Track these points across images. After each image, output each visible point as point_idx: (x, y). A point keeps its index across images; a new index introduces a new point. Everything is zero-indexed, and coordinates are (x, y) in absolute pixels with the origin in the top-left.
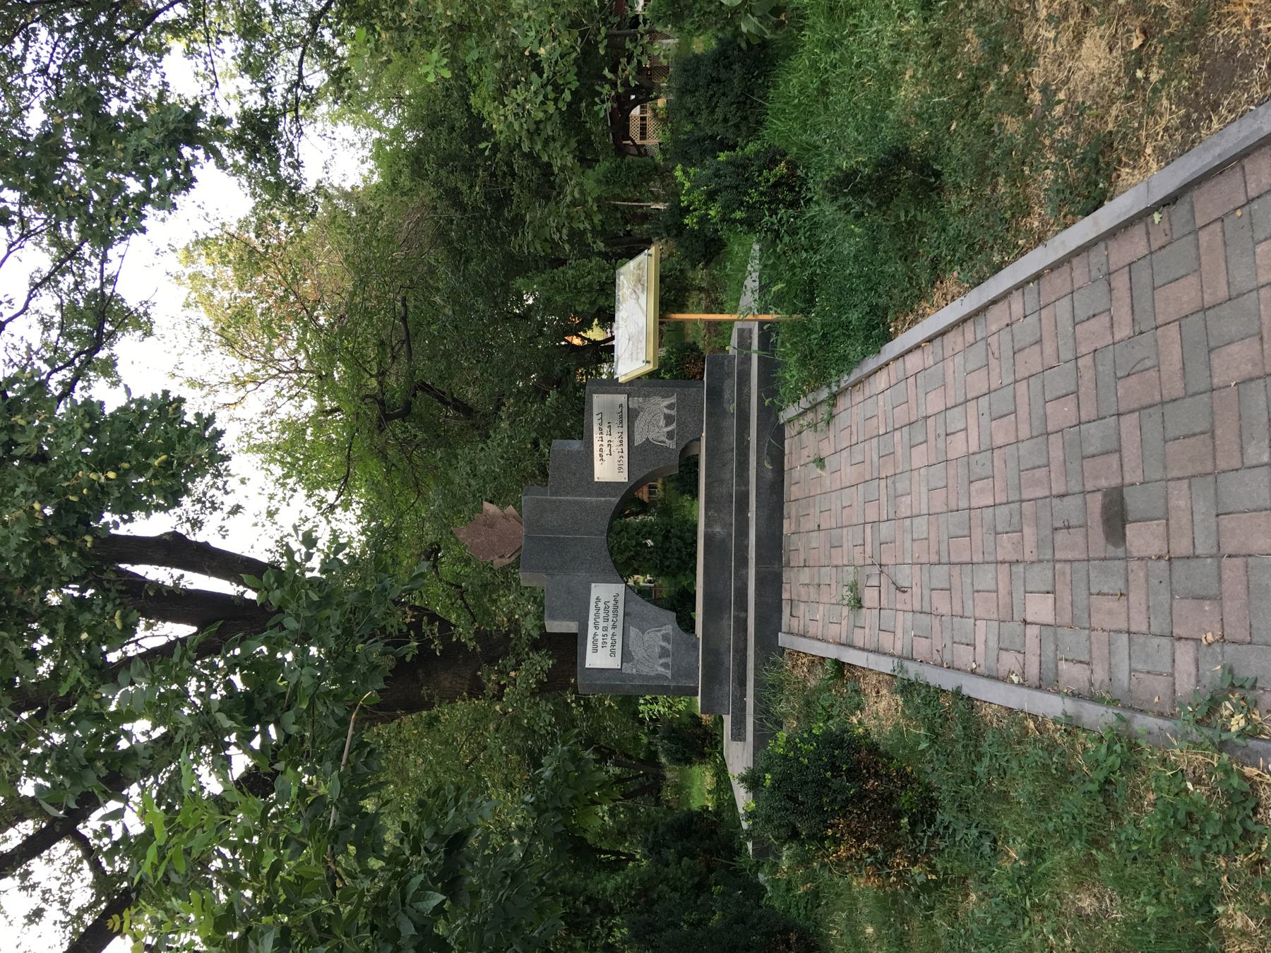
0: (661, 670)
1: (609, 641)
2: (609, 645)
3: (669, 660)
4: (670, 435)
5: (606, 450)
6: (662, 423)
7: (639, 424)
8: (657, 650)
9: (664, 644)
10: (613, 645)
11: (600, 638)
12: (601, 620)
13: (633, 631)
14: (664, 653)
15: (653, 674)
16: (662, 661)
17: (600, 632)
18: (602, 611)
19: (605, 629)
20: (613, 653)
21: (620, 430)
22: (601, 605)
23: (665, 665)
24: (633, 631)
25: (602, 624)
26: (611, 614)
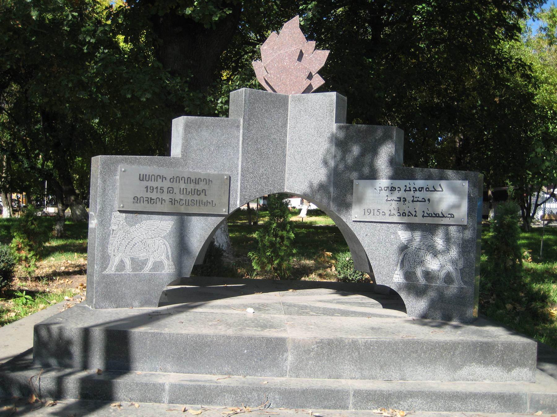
1: (154, 196)
2: (149, 195)
3: (128, 269)
8: (142, 256)
9: (150, 265)
10: (150, 200)
14: (138, 264)
15: (110, 250)
16: (128, 262)
17: (166, 184)
19: (170, 190)
21: (420, 214)
23: (121, 266)
26: (190, 198)
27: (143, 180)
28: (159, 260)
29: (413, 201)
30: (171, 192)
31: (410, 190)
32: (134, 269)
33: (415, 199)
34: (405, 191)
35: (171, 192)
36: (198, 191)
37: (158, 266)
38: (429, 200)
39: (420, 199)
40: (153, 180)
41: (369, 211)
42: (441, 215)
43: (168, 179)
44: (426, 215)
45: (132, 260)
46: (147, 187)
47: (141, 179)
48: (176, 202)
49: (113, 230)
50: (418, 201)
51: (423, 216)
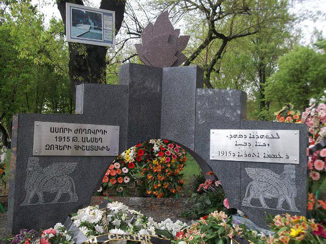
0: (32, 195)
1: (62, 144)
2: (58, 143)
3: (41, 201)
4: (255, 202)
5: (241, 141)
6: (268, 195)
7: (267, 173)
8: (53, 189)
9: (58, 196)
11: (66, 134)
12: (84, 135)
13: (73, 165)
14: (49, 196)
16: (41, 195)
17: (71, 135)
18: (93, 136)
20: (49, 147)
21: (262, 156)
22: (99, 135)
23: (36, 198)
24: (73, 165)
25: (79, 136)
27: (53, 132)
28: (66, 193)
29: (256, 145)
30: (76, 140)
31: (254, 137)
32: (46, 201)
33: (258, 144)
34: (250, 137)
35: (76, 140)
36: (96, 139)
37: (65, 197)
38: (268, 145)
39: (262, 144)
40: (61, 132)
41: (223, 153)
42: (278, 156)
43: (73, 131)
44: (266, 156)
45: (44, 193)
46: (56, 137)
47: (52, 131)
48: (79, 148)
49: (29, 171)
50: (260, 145)
51: (264, 157)
